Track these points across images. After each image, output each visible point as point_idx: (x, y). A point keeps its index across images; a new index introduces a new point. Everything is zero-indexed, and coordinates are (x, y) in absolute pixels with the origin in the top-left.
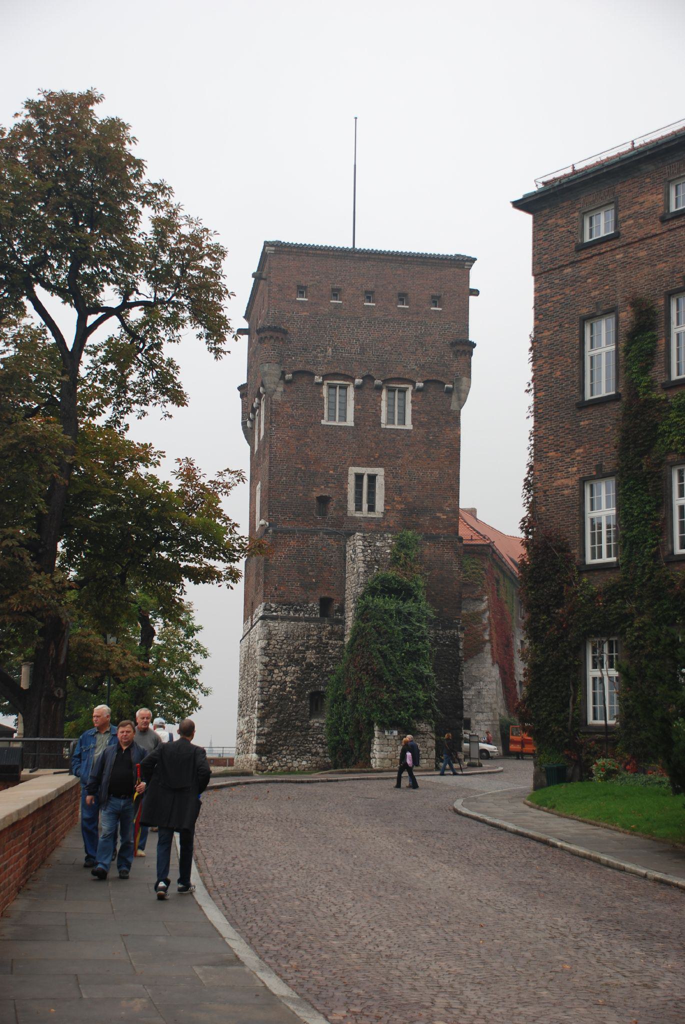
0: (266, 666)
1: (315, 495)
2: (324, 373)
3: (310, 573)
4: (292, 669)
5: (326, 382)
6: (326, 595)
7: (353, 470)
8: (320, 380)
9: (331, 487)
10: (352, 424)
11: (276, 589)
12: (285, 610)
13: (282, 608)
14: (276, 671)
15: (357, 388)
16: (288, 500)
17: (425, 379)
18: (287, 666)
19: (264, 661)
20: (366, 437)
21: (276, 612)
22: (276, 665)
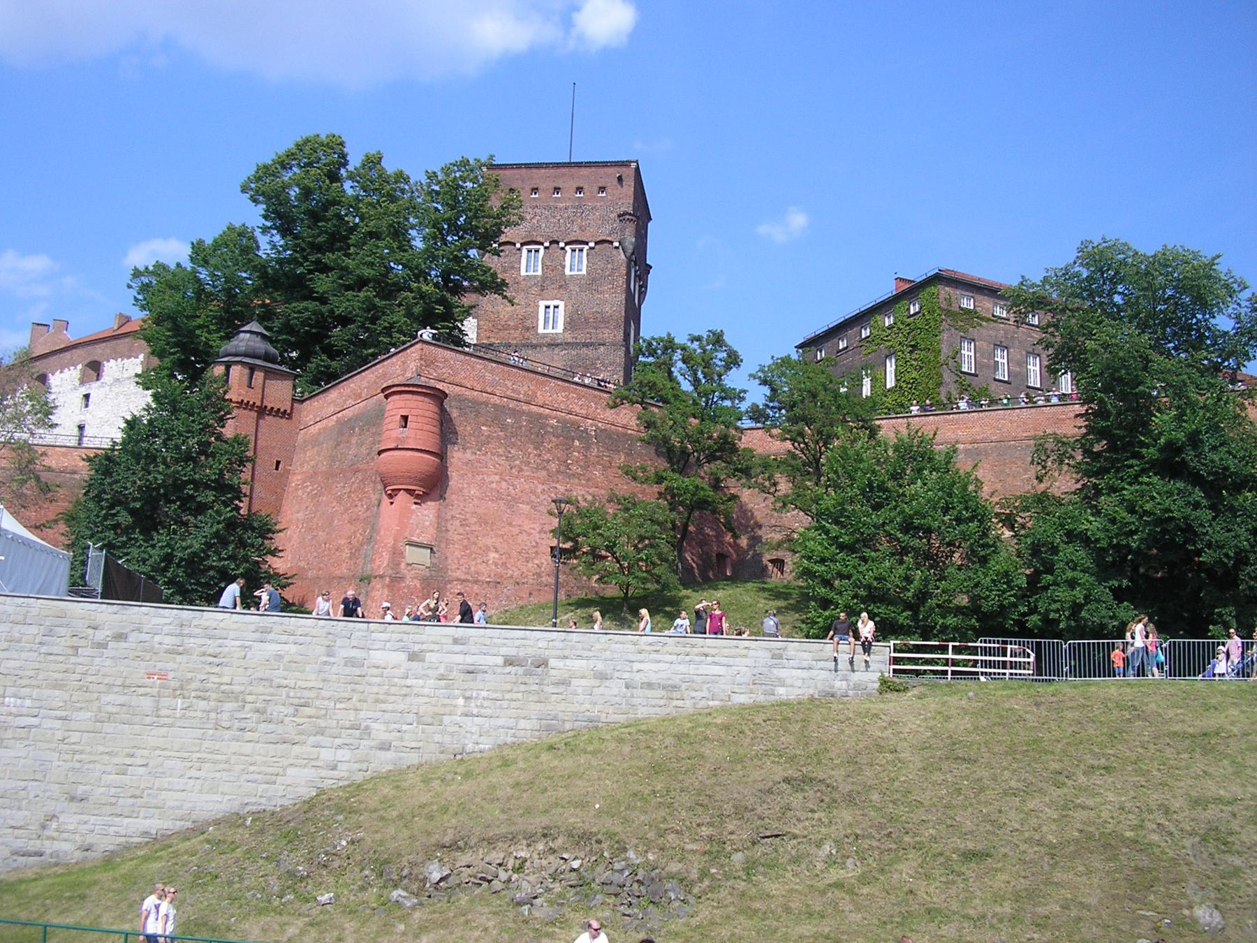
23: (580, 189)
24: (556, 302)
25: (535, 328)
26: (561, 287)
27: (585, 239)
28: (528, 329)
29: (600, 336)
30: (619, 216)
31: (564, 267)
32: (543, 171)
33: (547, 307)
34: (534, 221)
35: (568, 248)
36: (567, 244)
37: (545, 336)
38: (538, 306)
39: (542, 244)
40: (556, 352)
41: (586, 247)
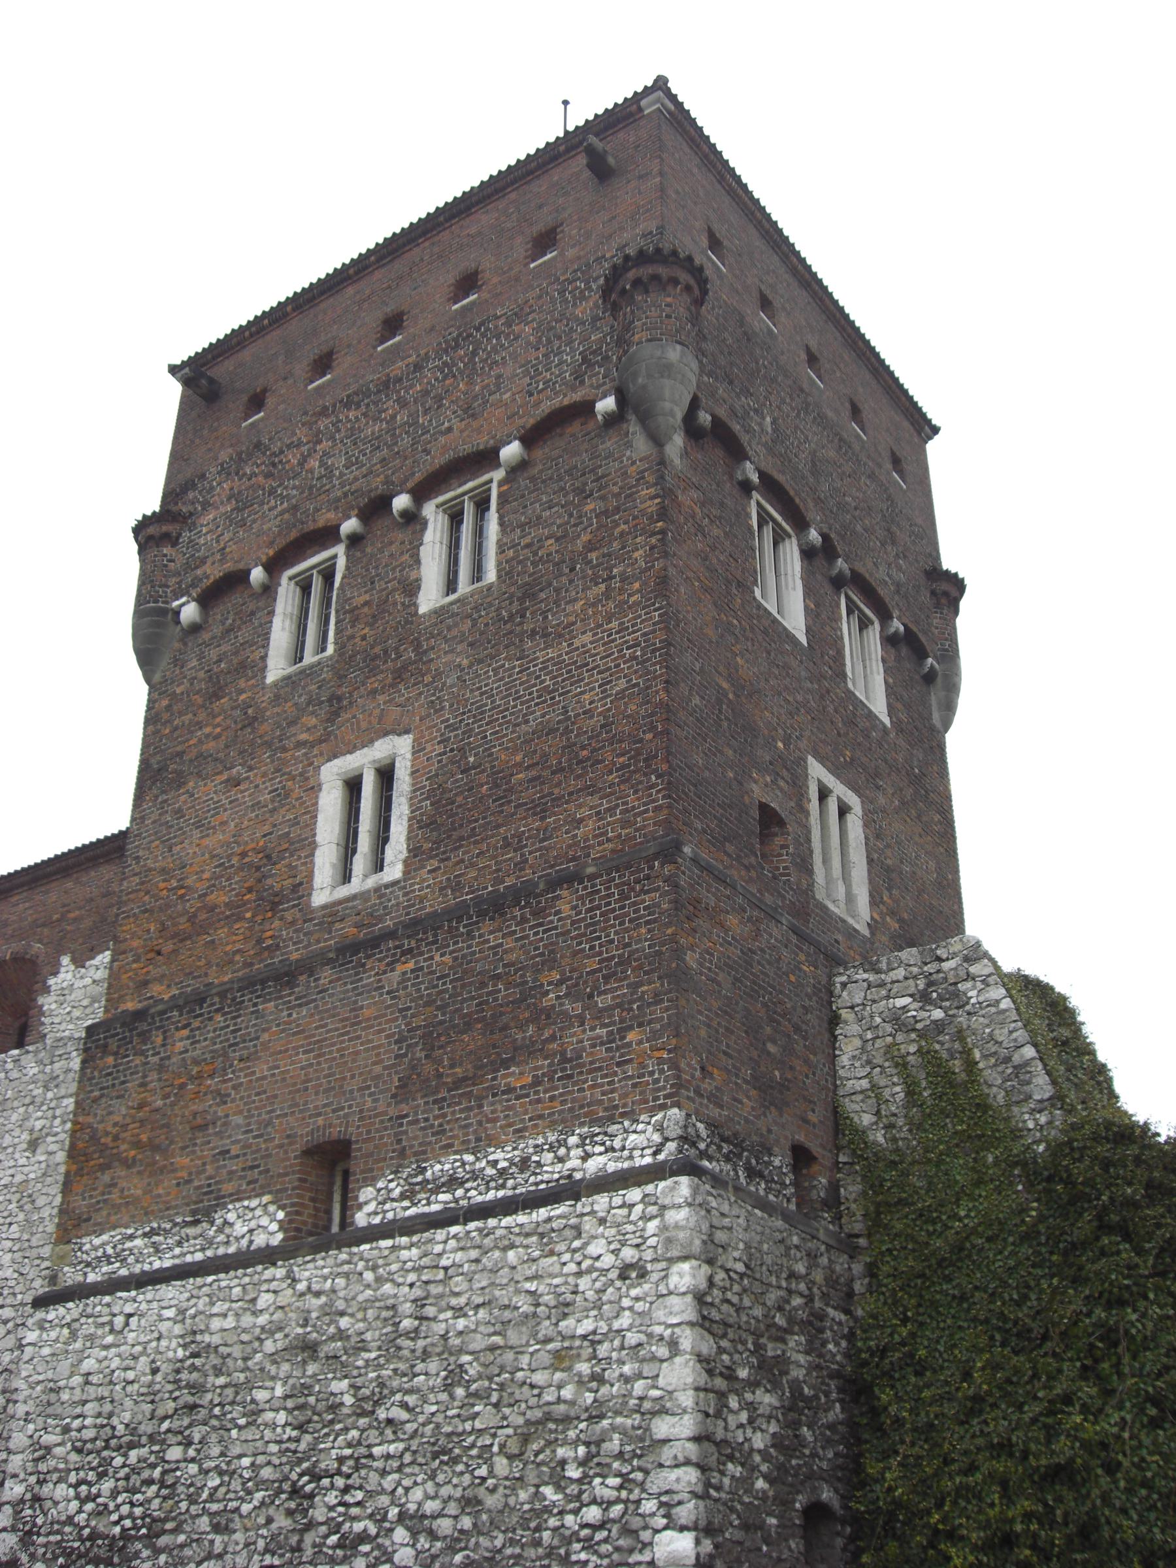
0: (710, 1372)
1: (759, 791)
2: (763, 466)
3: (771, 1048)
4: (766, 1399)
5: (755, 495)
6: (801, 1138)
7: (817, 770)
8: (755, 478)
9: (781, 790)
10: (804, 640)
11: (703, 1069)
12: (728, 1159)
13: (720, 1148)
14: (733, 1403)
15: (808, 554)
16: (707, 774)
17: (906, 621)
18: (753, 1384)
19: (705, 1350)
20: (828, 692)
21: (710, 1159)
22: (729, 1375)
23: (468, 283)
24: (380, 750)
25: (302, 887)
26: (399, 675)
27: (482, 442)
28: (274, 903)
29: (562, 840)
30: (606, 292)
31: (412, 589)
32: (350, 291)
33: (353, 786)
34: (314, 463)
35: (429, 510)
36: (421, 494)
37: (333, 911)
38: (316, 789)
39: (329, 535)
40: (369, 979)
41: (498, 475)
